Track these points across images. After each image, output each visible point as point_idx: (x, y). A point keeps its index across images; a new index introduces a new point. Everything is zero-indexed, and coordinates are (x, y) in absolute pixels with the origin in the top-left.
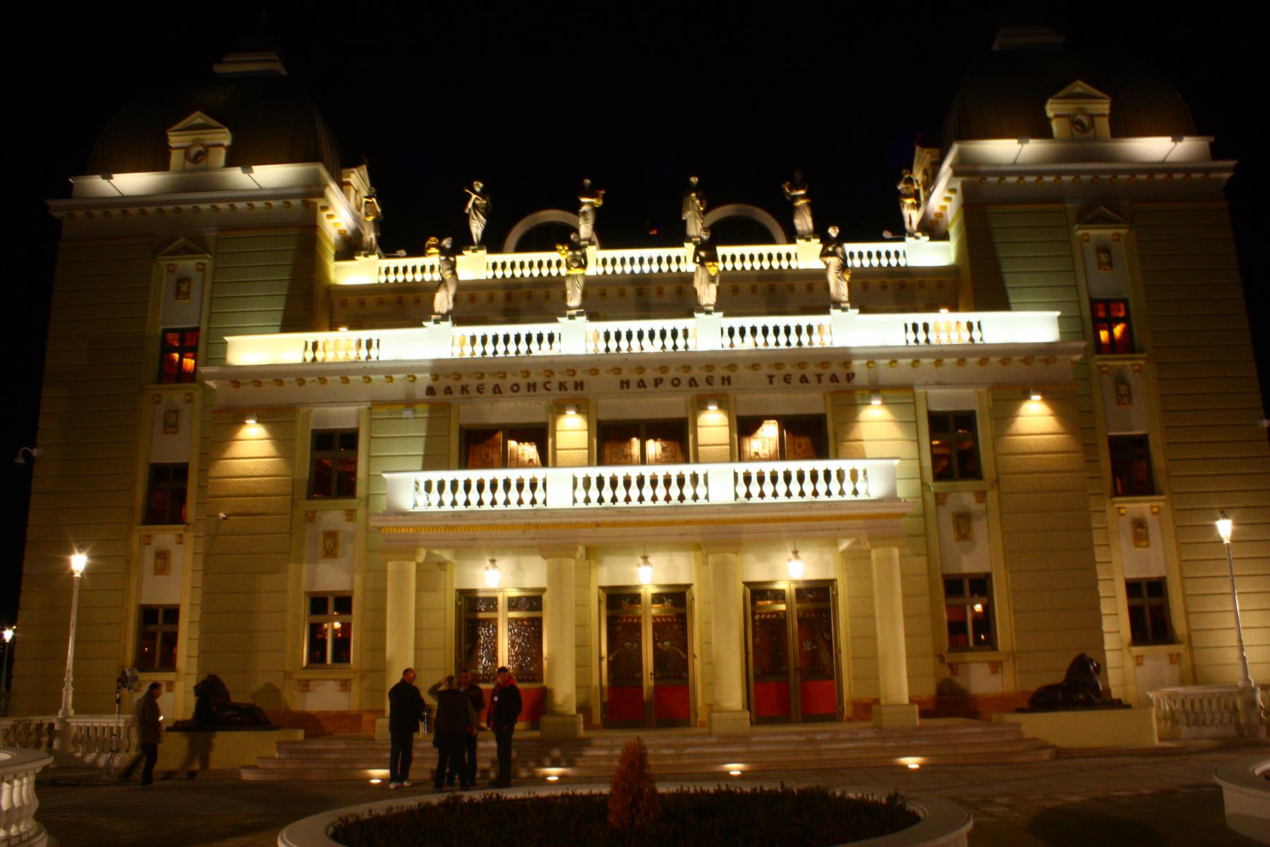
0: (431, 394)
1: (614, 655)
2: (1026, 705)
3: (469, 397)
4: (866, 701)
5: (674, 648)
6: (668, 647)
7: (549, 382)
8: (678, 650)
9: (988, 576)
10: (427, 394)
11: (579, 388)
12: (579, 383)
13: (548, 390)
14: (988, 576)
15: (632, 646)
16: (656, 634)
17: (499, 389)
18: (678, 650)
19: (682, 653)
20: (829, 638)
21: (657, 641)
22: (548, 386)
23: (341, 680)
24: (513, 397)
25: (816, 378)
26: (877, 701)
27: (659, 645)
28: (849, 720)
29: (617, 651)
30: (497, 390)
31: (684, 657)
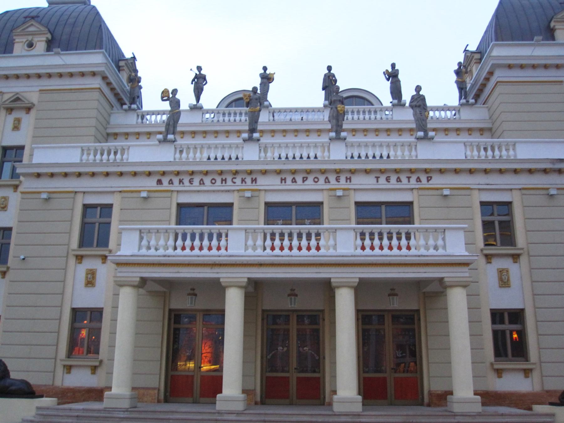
0: (160, 184)
1: (271, 355)
2: (555, 400)
3: (184, 186)
4: (440, 392)
5: (310, 351)
6: (306, 351)
7: (235, 178)
8: (313, 353)
9: (522, 310)
10: (157, 184)
11: (254, 182)
12: (253, 179)
13: (235, 183)
14: (522, 310)
15: (283, 350)
16: (299, 342)
17: (203, 182)
18: (313, 353)
19: (315, 355)
20: (413, 349)
21: (299, 347)
22: (234, 180)
23: (91, 366)
24: (211, 186)
25: (407, 179)
26: (451, 393)
27: (301, 349)
28: (429, 405)
29: (273, 352)
30: (202, 182)
31: (317, 358)
